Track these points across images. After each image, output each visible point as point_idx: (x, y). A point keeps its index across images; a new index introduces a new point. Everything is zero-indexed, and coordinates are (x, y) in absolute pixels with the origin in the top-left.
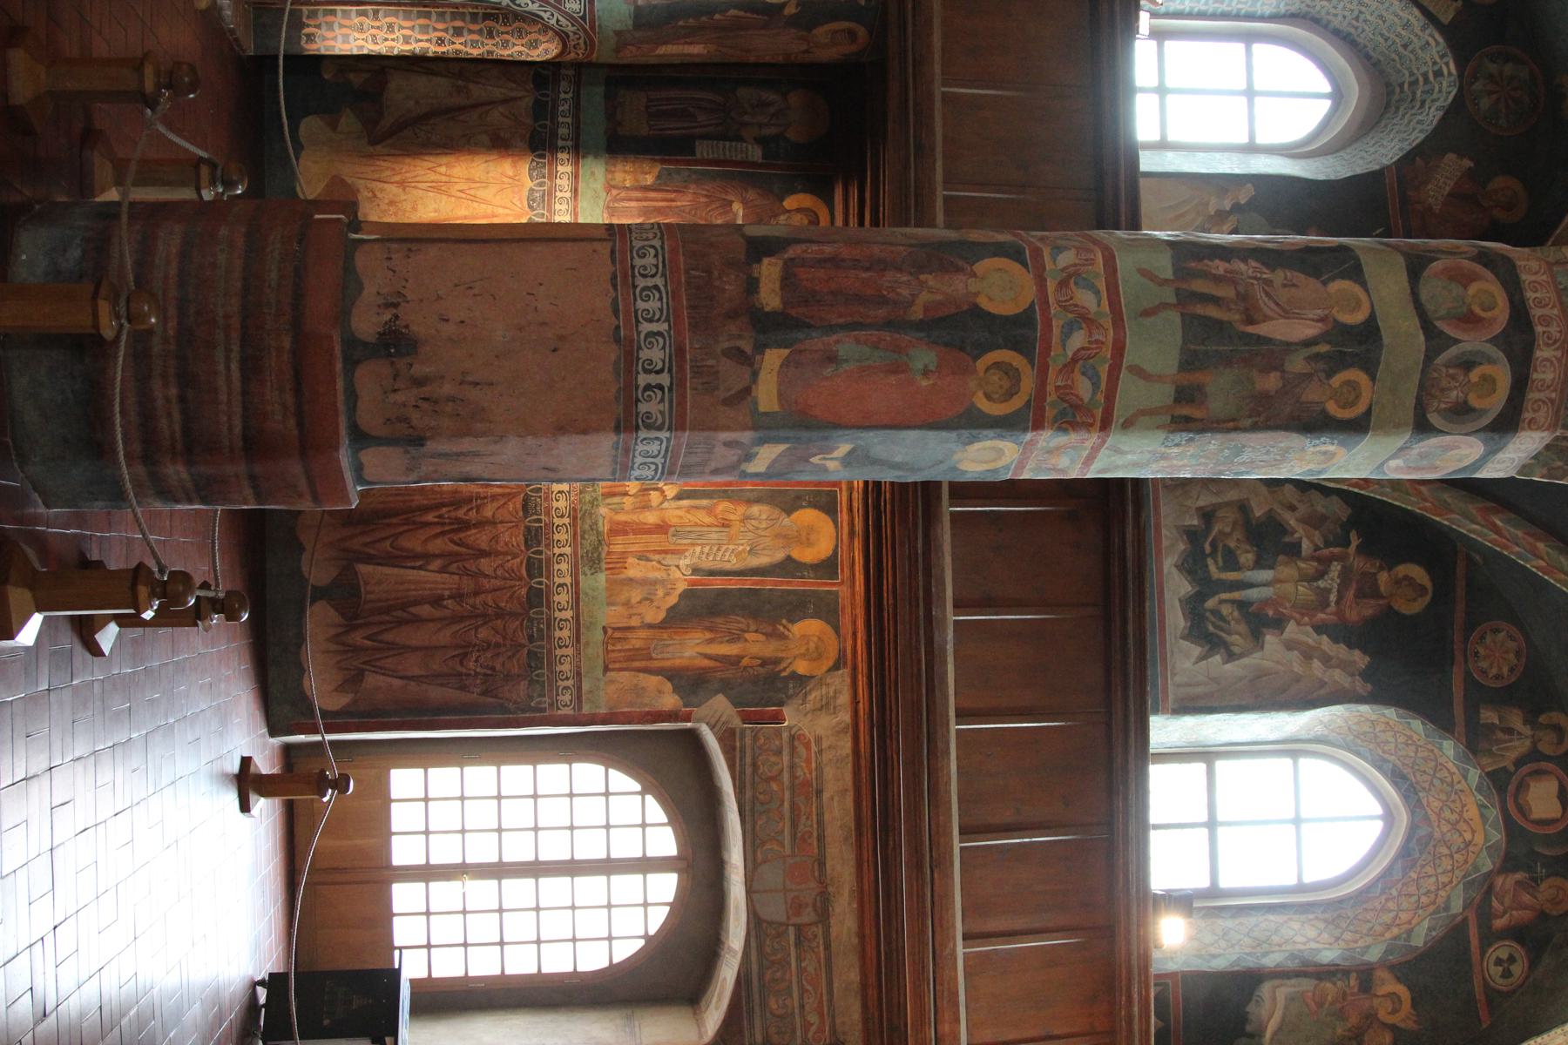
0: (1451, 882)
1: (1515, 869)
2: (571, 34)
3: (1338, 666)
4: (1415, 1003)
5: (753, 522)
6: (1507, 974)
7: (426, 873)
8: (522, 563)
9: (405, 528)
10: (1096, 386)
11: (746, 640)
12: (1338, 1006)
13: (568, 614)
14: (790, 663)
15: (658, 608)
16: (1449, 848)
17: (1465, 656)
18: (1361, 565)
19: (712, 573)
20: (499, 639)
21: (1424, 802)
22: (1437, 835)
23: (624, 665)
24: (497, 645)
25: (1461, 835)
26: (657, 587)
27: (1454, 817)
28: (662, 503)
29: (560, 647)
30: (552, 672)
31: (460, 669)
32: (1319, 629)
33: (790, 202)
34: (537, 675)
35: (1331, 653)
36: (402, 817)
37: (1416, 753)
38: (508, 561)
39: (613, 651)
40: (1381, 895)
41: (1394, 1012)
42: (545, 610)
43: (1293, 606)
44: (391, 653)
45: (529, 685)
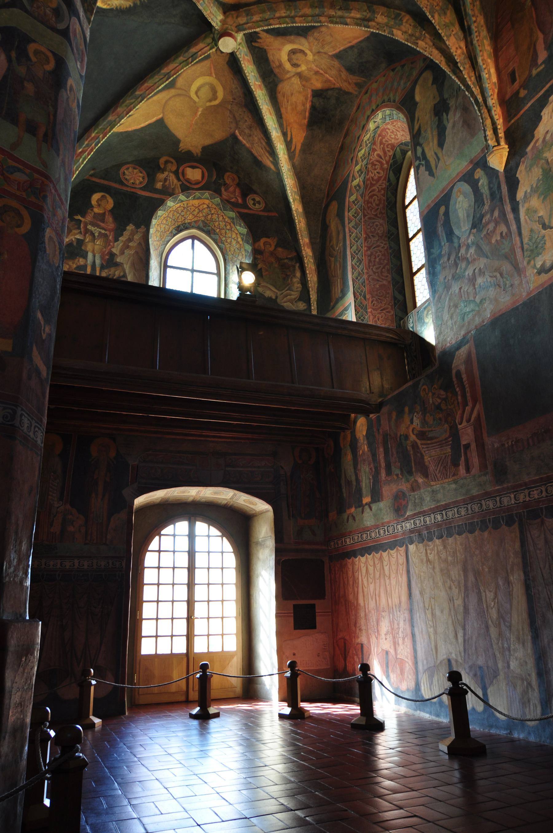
0: (222, 216)
1: (221, 191)
3: (133, 236)
4: (269, 237)
6: (259, 203)
7: (190, 637)
10: (19, 170)
12: (267, 264)
16: (209, 215)
17: (133, 188)
18: (89, 217)
21: (189, 221)
22: (203, 219)
25: (204, 209)
27: (197, 210)
32: (116, 240)
35: (127, 238)
36: (164, 649)
37: (170, 218)
40: (224, 244)
41: (270, 244)
43: (105, 248)
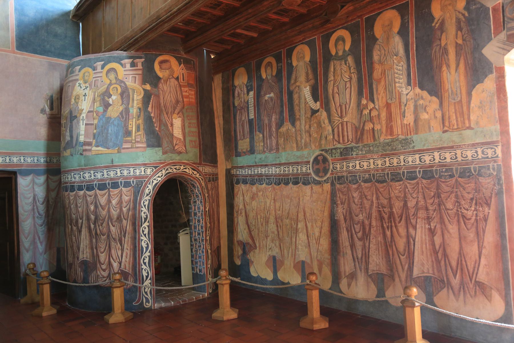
2: (168, 171)
5: (382, 58)
8: (409, 183)
9: (394, 247)
11: (446, 44)
13: (436, 154)
14: (459, 12)
15: (430, 102)
19: (409, 75)
20: (453, 195)
23: (466, 117)
24: (457, 196)
26: (418, 104)
28: (376, 109)
29: (456, 158)
30: (473, 162)
31: (473, 220)
33: (264, 77)
34: (475, 171)
38: (409, 191)
39: (457, 125)
42: (434, 169)
44: (464, 263)
45: (481, 176)
